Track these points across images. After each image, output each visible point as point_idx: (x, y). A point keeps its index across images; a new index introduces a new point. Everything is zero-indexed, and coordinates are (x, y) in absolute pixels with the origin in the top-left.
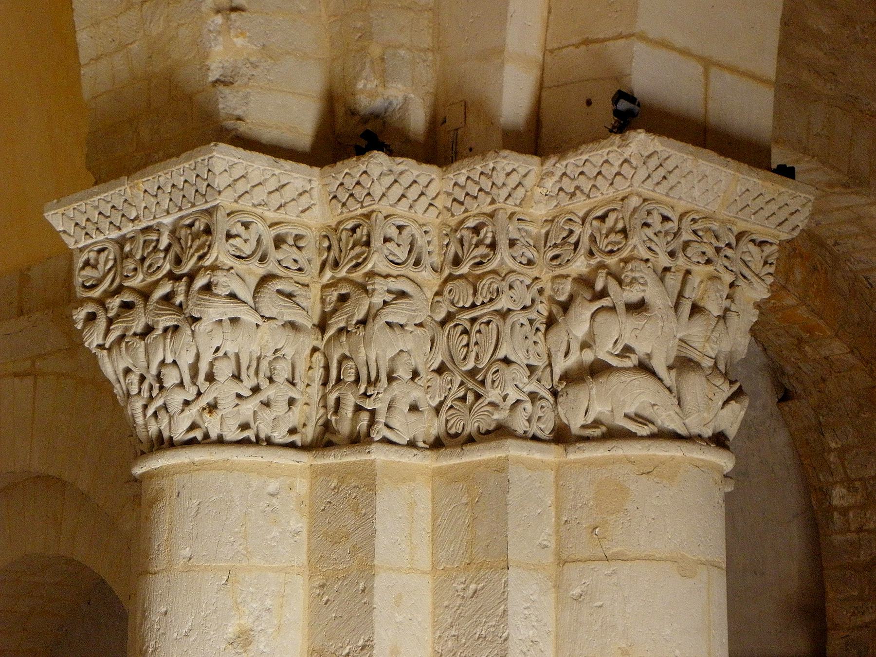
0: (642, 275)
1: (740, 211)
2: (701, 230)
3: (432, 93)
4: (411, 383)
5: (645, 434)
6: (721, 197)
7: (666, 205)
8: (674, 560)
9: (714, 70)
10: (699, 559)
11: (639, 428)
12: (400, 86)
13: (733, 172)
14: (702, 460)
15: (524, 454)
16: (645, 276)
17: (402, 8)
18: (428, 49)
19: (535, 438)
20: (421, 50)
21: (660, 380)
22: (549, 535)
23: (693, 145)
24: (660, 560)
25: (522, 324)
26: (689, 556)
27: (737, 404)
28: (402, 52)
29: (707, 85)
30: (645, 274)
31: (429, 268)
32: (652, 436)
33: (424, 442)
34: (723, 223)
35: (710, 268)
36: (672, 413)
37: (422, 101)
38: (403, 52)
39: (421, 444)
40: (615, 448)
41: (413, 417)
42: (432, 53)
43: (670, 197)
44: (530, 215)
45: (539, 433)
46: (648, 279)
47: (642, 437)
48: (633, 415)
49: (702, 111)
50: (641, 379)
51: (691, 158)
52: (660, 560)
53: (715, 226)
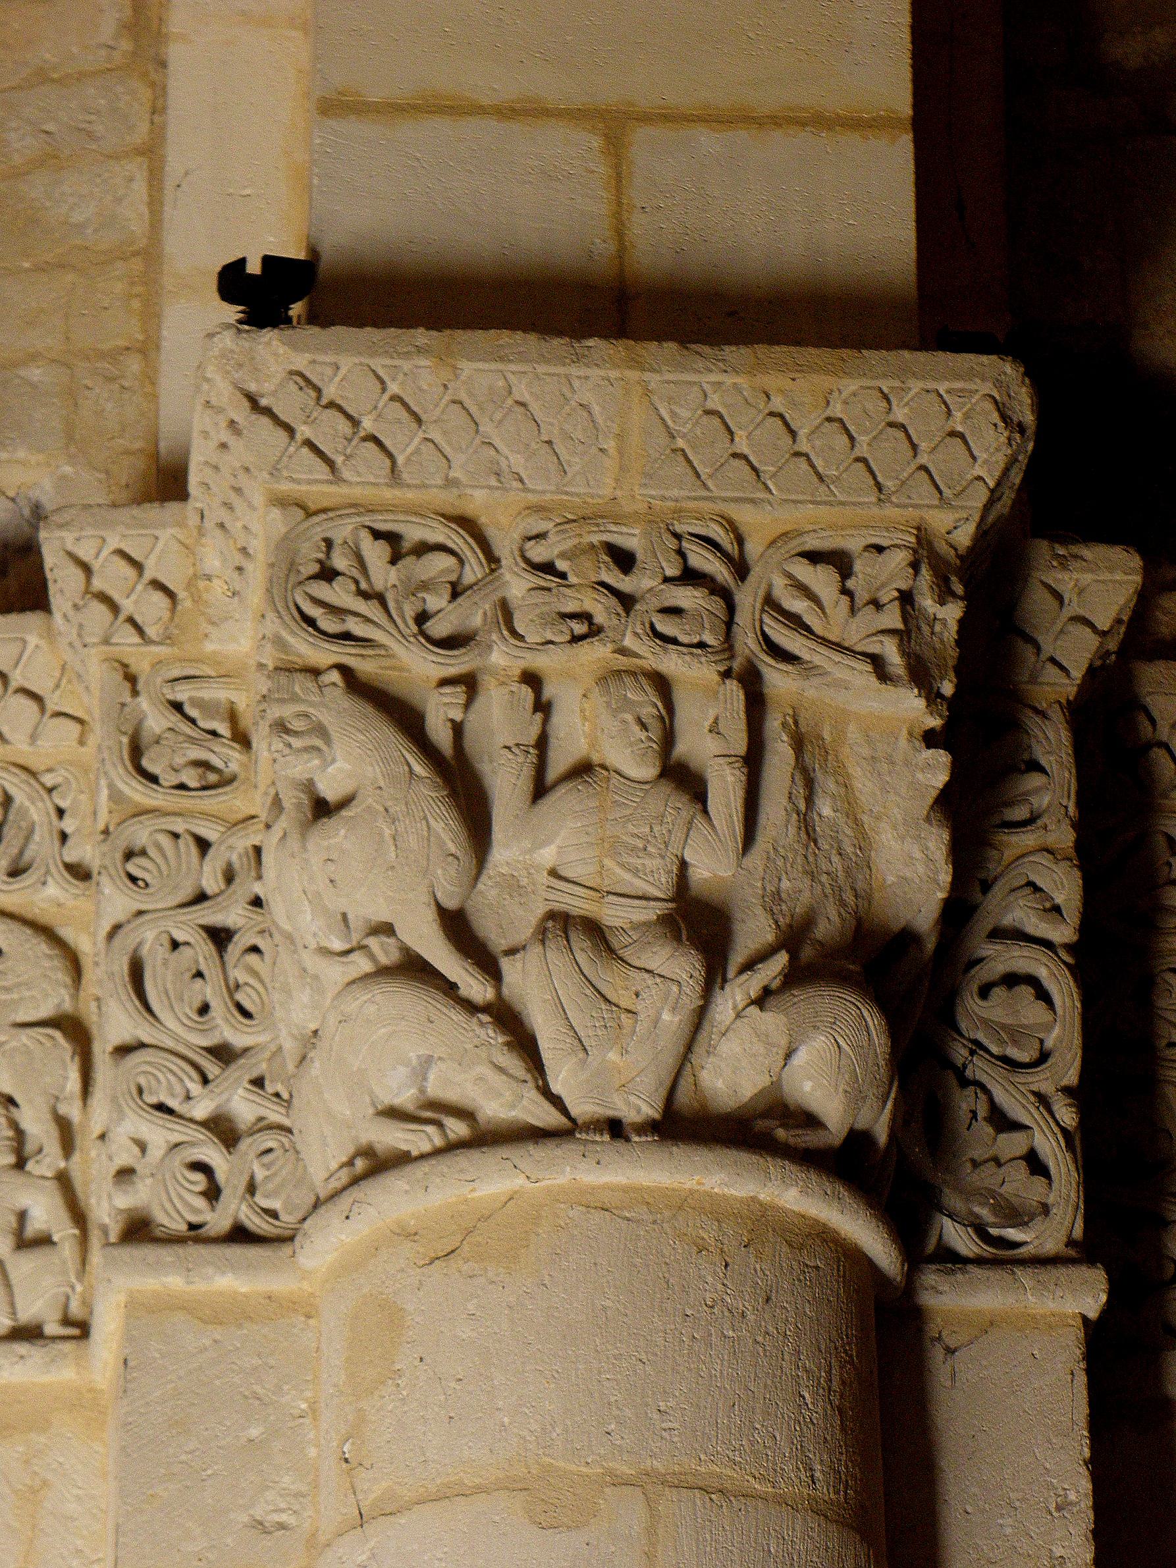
0: (302, 708)
1: (290, 430)
2: (563, 555)
3: (141, 451)
4: (16, 1178)
5: (426, 1147)
6: (612, 452)
7: (406, 512)
8: (520, 1486)
9: (641, 138)
10: (611, 1473)
11: (410, 1136)
12: (21, 454)
13: (614, 374)
14: (625, 1189)
15: (174, 1282)
16: (311, 710)
17: (39, 269)
18: (128, 349)
19: (240, 1235)
20: (103, 355)
21: (449, 989)
22: (298, 1495)
23: (428, 328)
24: (480, 1490)
25: (175, 945)
26: (573, 1467)
27: (764, 1015)
28: (35, 373)
29: (619, 181)
30: (312, 704)
31: (59, 873)
32: (453, 1147)
33: (66, 1321)
34: (649, 518)
35: (597, 653)
36: (485, 1070)
37: (103, 476)
38: (38, 372)
39: (51, 1329)
40: (355, 1209)
41: (22, 1267)
42: (139, 356)
43: (408, 486)
44: (214, 659)
45: (257, 1220)
46: (325, 718)
47: (423, 1157)
48: (410, 1107)
49: (612, 247)
50: (379, 998)
51: (423, 362)
52: (480, 1490)
53: (631, 539)
